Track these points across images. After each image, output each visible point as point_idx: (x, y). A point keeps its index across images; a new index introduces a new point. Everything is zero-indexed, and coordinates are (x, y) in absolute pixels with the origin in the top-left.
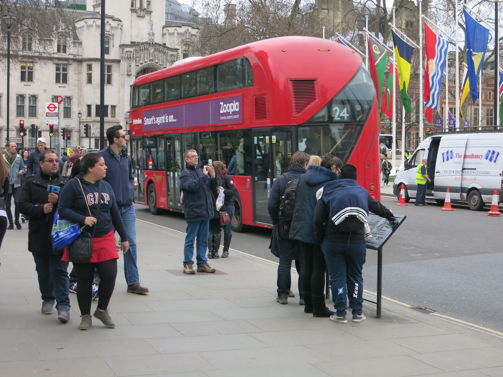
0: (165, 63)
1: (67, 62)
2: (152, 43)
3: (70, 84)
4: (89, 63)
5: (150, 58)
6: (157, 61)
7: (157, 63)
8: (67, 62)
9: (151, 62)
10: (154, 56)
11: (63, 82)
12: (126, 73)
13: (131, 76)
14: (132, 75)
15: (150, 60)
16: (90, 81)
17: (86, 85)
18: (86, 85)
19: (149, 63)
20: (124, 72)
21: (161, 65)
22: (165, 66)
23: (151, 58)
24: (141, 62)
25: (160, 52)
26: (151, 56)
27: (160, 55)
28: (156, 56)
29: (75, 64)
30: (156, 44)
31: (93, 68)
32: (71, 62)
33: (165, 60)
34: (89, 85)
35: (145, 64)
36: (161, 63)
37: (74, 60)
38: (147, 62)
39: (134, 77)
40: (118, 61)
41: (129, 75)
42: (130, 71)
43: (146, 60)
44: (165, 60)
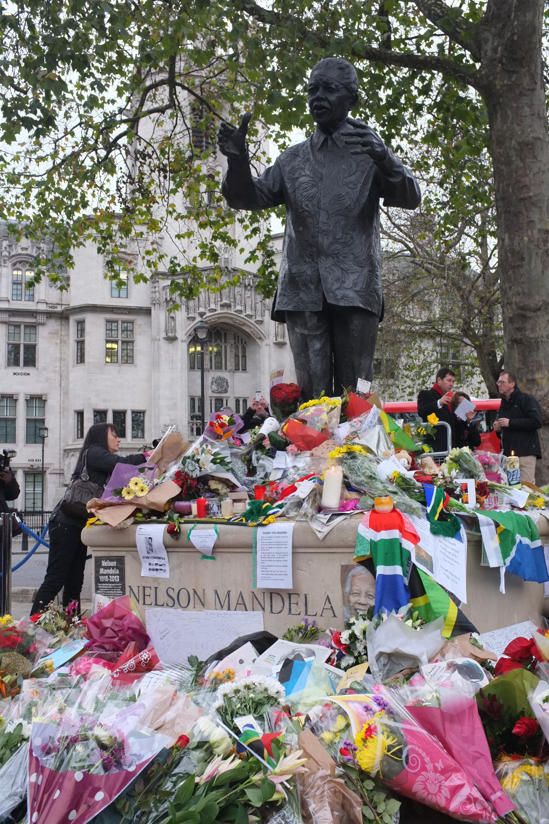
0: (259, 313)
1: (33, 320)
2: (227, 268)
3: (40, 368)
4: (79, 317)
5: (221, 300)
6: (239, 308)
7: (240, 312)
8: (33, 320)
9: (225, 310)
10: (232, 296)
11: (26, 364)
12: (163, 335)
13: (175, 342)
14: (180, 339)
15: (222, 306)
16: (81, 358)
17: (74, 366)
18: (74, 366)
19: (219, 311)
20: (158, 334)
21: (250, 316)
22: (259, 318)
23: (224, 301)
24: (202, 310)
25: (246, 287)
26: (224, 298)
27: (248, 294)
28: (238, 297)
29: (53, 325)
30: (234, 270)
31: (88, 327)
32: (41, 319)
33: (259, 306)
34: (81, 366)
35: (208, 314)
36: (249, 312)
37: (50, 315)
38: (215, 310)
39: (185, 345)
40: (147, 312)
41: (172, 339)
42: (174, 330)
43: (213, 306)
44: (259, 306)
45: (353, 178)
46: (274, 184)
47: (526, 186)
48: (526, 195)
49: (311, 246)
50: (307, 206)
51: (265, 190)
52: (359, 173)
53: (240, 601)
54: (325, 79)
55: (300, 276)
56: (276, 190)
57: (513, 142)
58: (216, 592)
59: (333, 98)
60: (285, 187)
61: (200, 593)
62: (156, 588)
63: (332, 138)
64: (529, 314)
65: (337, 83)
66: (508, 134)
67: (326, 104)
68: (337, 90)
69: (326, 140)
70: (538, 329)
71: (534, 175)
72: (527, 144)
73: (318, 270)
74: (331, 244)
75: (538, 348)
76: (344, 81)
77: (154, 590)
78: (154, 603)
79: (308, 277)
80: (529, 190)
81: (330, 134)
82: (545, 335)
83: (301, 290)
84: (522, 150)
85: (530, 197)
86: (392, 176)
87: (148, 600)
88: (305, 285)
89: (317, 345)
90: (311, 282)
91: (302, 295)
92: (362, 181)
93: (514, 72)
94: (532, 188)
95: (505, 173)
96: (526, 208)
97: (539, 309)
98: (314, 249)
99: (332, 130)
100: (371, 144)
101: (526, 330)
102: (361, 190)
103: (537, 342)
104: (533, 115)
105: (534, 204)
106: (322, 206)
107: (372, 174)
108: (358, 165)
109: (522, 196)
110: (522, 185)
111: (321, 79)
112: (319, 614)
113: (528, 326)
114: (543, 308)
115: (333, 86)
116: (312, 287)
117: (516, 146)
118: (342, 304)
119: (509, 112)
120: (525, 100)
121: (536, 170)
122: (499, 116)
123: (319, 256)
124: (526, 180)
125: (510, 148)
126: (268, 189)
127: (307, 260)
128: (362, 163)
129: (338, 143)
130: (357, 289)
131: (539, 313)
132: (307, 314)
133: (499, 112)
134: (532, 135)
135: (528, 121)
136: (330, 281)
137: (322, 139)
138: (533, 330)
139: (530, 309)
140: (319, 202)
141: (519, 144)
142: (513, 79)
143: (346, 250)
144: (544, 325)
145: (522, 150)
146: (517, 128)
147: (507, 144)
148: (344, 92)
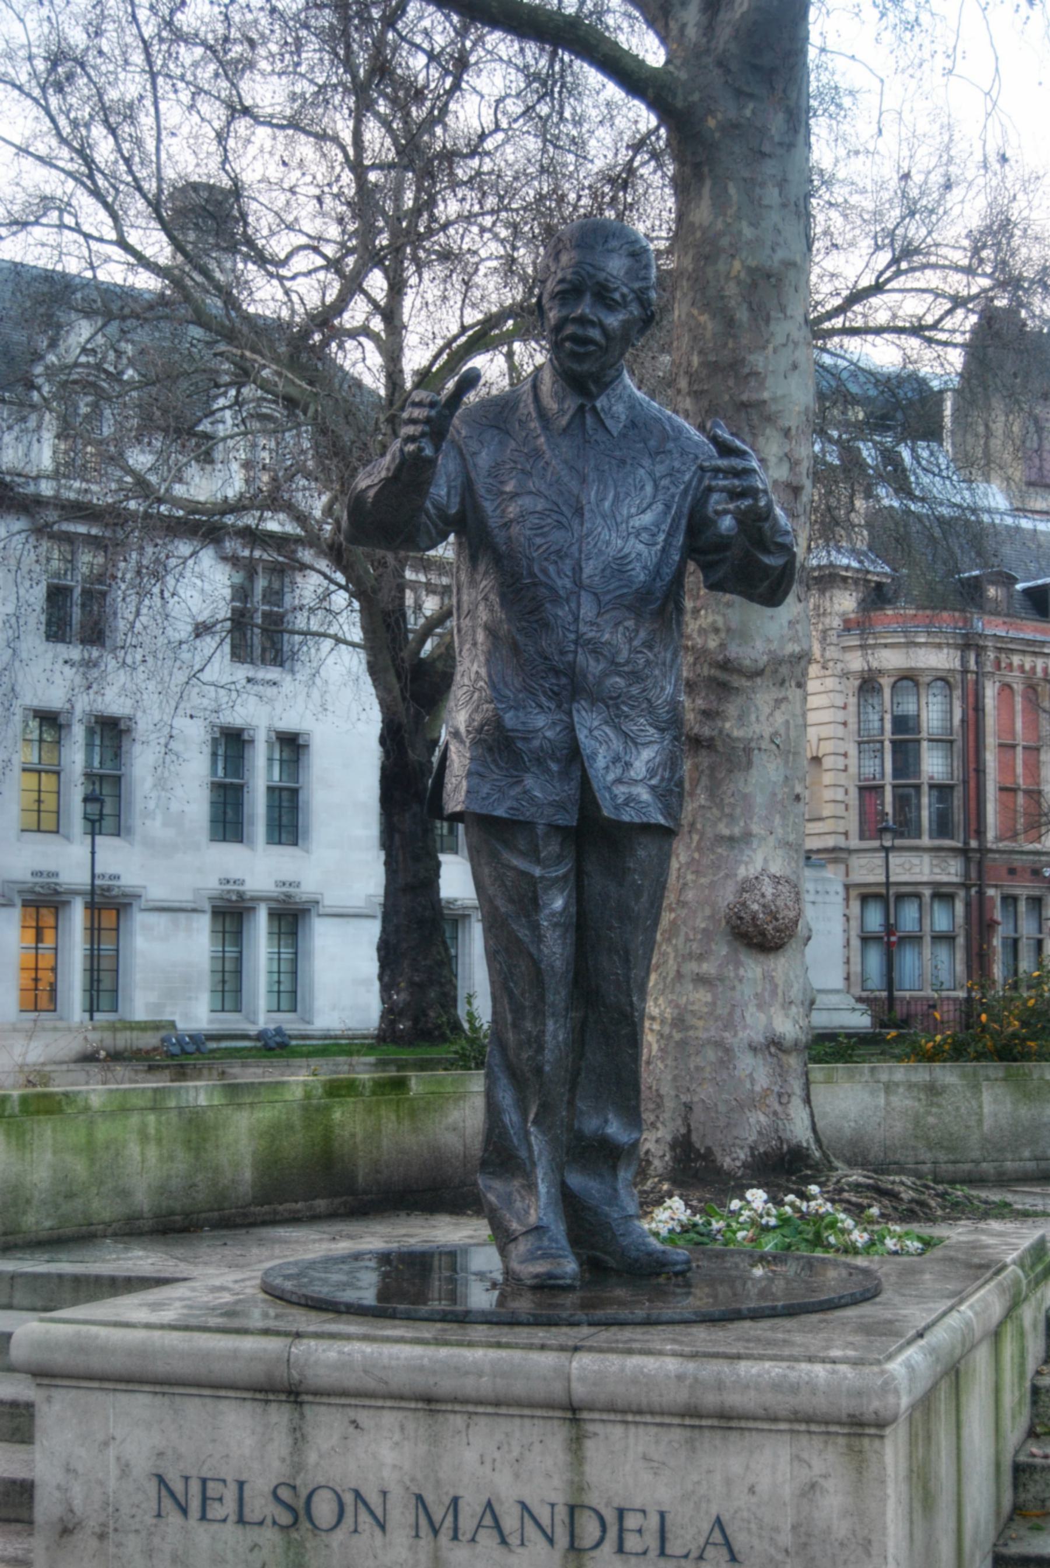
45: (648, 518)
46: (449, 494)
47: (758, 374)
48: (754, 396)
49: (557, 673)
50: (545, 571)
51: (432, 511)
52: (659, 507)
53: (488, 1521)
54: (602, 276)
55: (524, 739)
56: (453, 511)
57: (737, 265)
58: (419, 1498)
59: (613, 321)
60: (477, 508)
61: (374, 1499)
62: (241, 1484)
63: (594, 409)
64: (737, 681)
65: (625, 290)
66: (725, 242)
67: (595, 333)
68: (624, 304)
69: (581, 409)
70: (753, 718)
71: (775, 351)
72: (769, 276)
73: (571, 729)
74: (605, 674)
75: (750, 764)
76: (637, 285)
77: (233, 1487)
78: (233, 1518)
79: (546, 745)
80: (762, 385)
81: (592, 397)
82: (766, 735)
83: (527, 770)
84: (754, 285)
85: (764, 402)
86: (767, 551)
87: (216, 1511)
88: (539, 762)
89: (558, 904)
90: (553, 757)
91: (529, 781)
92: (665, 527)
93: (751, 96)
94: (770, 382)
95: (708, 335)
96: (752, 427)
97: (759, 673)
98: (564, 681)
99: (593, 388)
100: (751, 492)
101: (725, 719)
102: (663, 550)
103: (748, 751)
104: (784, 206)
105: (769, 419)
106: (586, 582)
107: (686, 510)
108: (656, 486)
109: (744, 397)
110: (746, 370)
111: (591, 277)
112: (694, 1554)
113: (732, 709)
114: (768, 671)
115: (617, 296)
116: (554, 767)
117: (743, 275)
118: (626, 818)
119: (732, 190)
120: (769, 168)
121: (779, 339)
122: (706, 190)
123: (573, 698)
124: (757, 360)
125: (728, 277)
126: (434, 506)
127: (543, 700)
128: (665, 482)
129: (608, 423)
130: (653, 782)
131: (759, 680)
132: (540, 830)
133: (708, 184)
134: (780, 254)
135: (774, 217)
136: (601, 762)
137: (571, 404)
138: (742, 719)
139: (740, 671)
140: (578, 569)
141: (751, 271)
142: (748, 113)
143: (635, 690)
144: (767, 710)
145: (754, 285)
146: (748, 232)
147: (721, 266)
148: (635, 310)
